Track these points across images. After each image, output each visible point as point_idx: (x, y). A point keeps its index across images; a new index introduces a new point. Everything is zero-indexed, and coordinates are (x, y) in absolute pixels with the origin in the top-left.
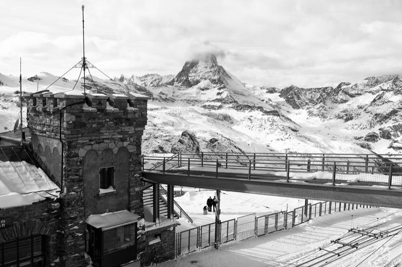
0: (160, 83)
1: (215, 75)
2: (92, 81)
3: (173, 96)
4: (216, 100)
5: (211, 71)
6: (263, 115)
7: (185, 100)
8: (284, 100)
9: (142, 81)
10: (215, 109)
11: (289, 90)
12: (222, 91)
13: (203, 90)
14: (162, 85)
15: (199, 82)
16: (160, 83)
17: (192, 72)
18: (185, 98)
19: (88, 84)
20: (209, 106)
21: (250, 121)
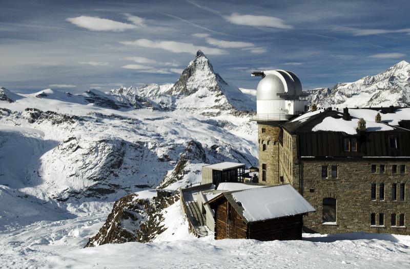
0: (159, 93)
2: (95, 95)
3: (172, 105)
4: (214, 106)
5: (208, 79)
7: (184, 108)
10: (214, 116)
12: (220, 97)
13: (201, 98)
14: (160, 96)
15: (197, 90)
19: (91, 98)
20: (208, 113)
21: (249, 127)
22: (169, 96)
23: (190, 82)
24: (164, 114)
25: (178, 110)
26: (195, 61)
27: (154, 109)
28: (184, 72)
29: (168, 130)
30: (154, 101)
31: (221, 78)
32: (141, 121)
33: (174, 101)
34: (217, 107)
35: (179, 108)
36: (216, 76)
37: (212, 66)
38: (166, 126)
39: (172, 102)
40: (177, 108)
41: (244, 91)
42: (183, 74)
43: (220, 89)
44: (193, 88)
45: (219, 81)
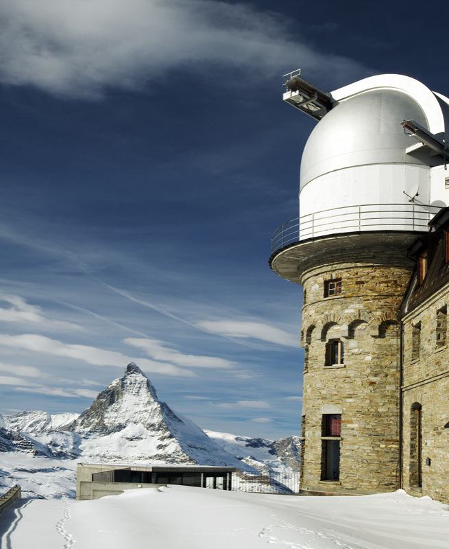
0: (48, 427)
1: (153, 417)
3: (73, 448)
4: (156, 456)
5: (146, 411)
6: (241, 482)
7: (97, 455)
8: (279, 459)
9: (12, 422)
11: (286, 444)
12: (166, 442)
13: (132, 440)
14: (50, 432)
15: (124, 427)
16: (48, 427)
17: (112, 411)
18: (97, 453)
22: (68, 433)
23: (111, 413)
24: (56, 463)
25: (85, 457)
26: (122, 380)
27: (37, 453)
28: (100, 395)
29: (62, 490)
30: (37, 439)
31: (170, 411)
32: (7, 473)
33: (77, 443)
34: (160, 457)
35: (88, 454)
36: (162, 407)
37: (154, 391)
38: (58, 484)
39: (75, 443)
40: (82, 454)
41: (212, 434)
42: (98, 398)
43: (167, 428)
44: (116, 423)
45: (167, 415)
